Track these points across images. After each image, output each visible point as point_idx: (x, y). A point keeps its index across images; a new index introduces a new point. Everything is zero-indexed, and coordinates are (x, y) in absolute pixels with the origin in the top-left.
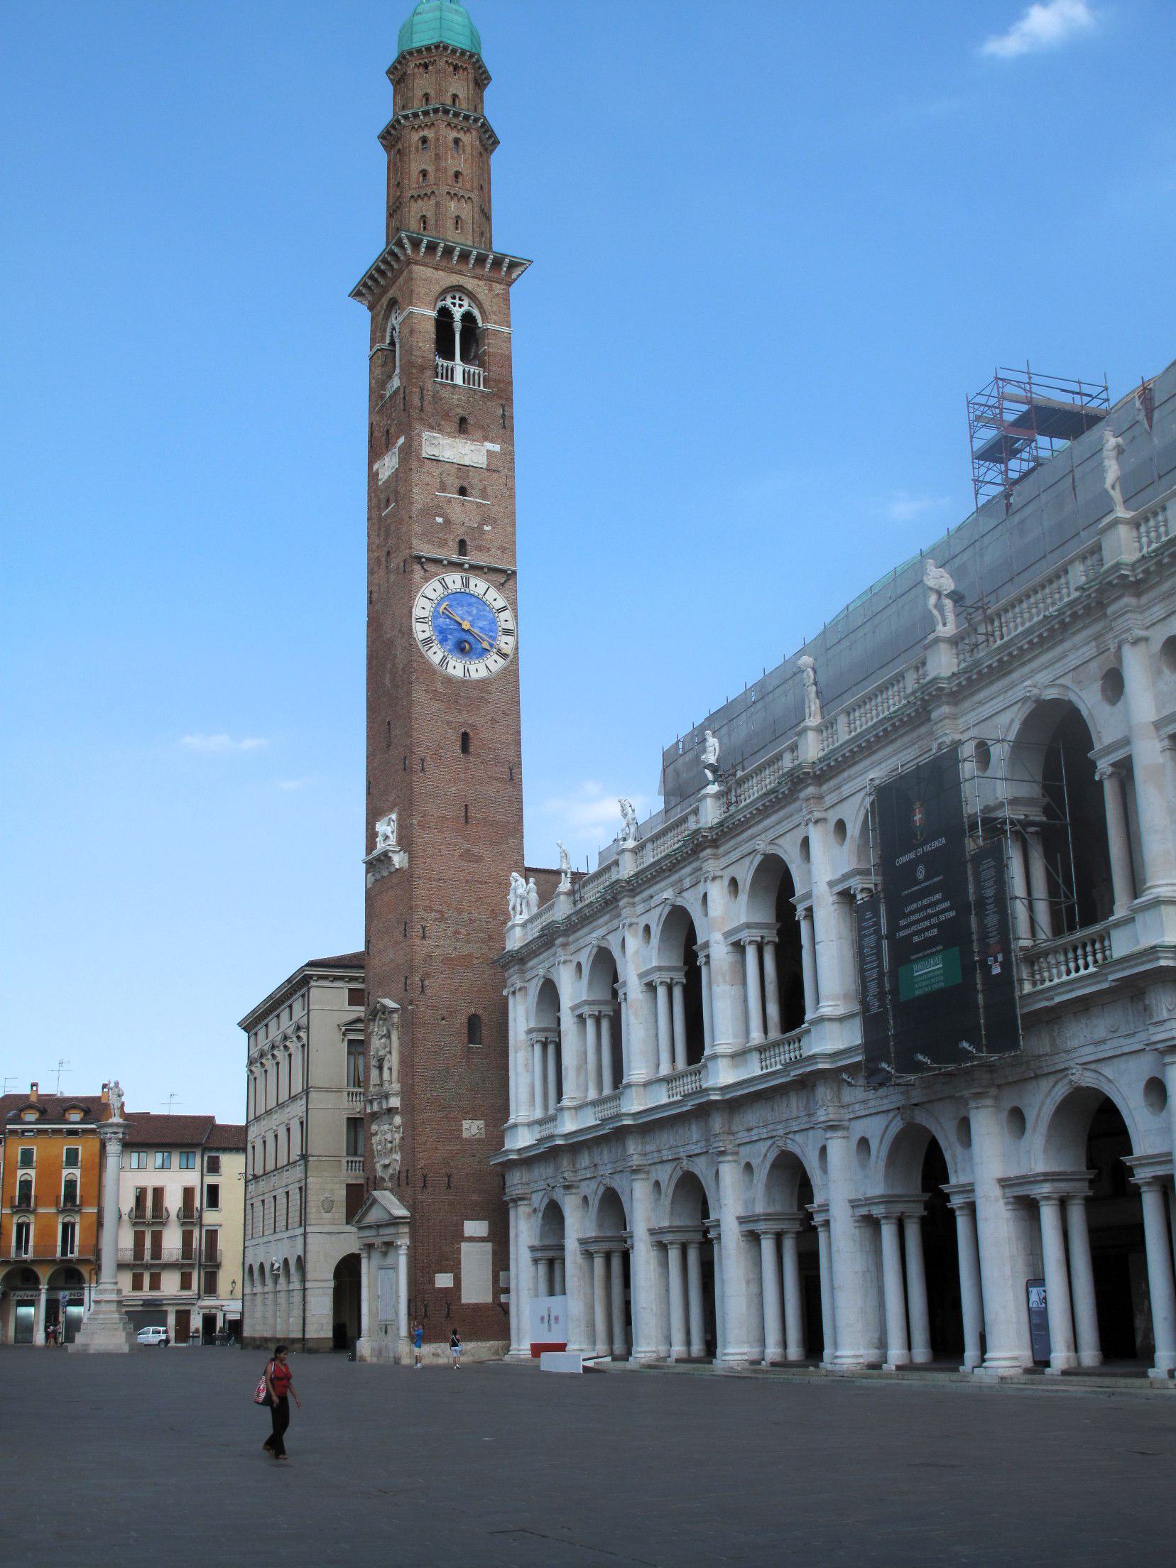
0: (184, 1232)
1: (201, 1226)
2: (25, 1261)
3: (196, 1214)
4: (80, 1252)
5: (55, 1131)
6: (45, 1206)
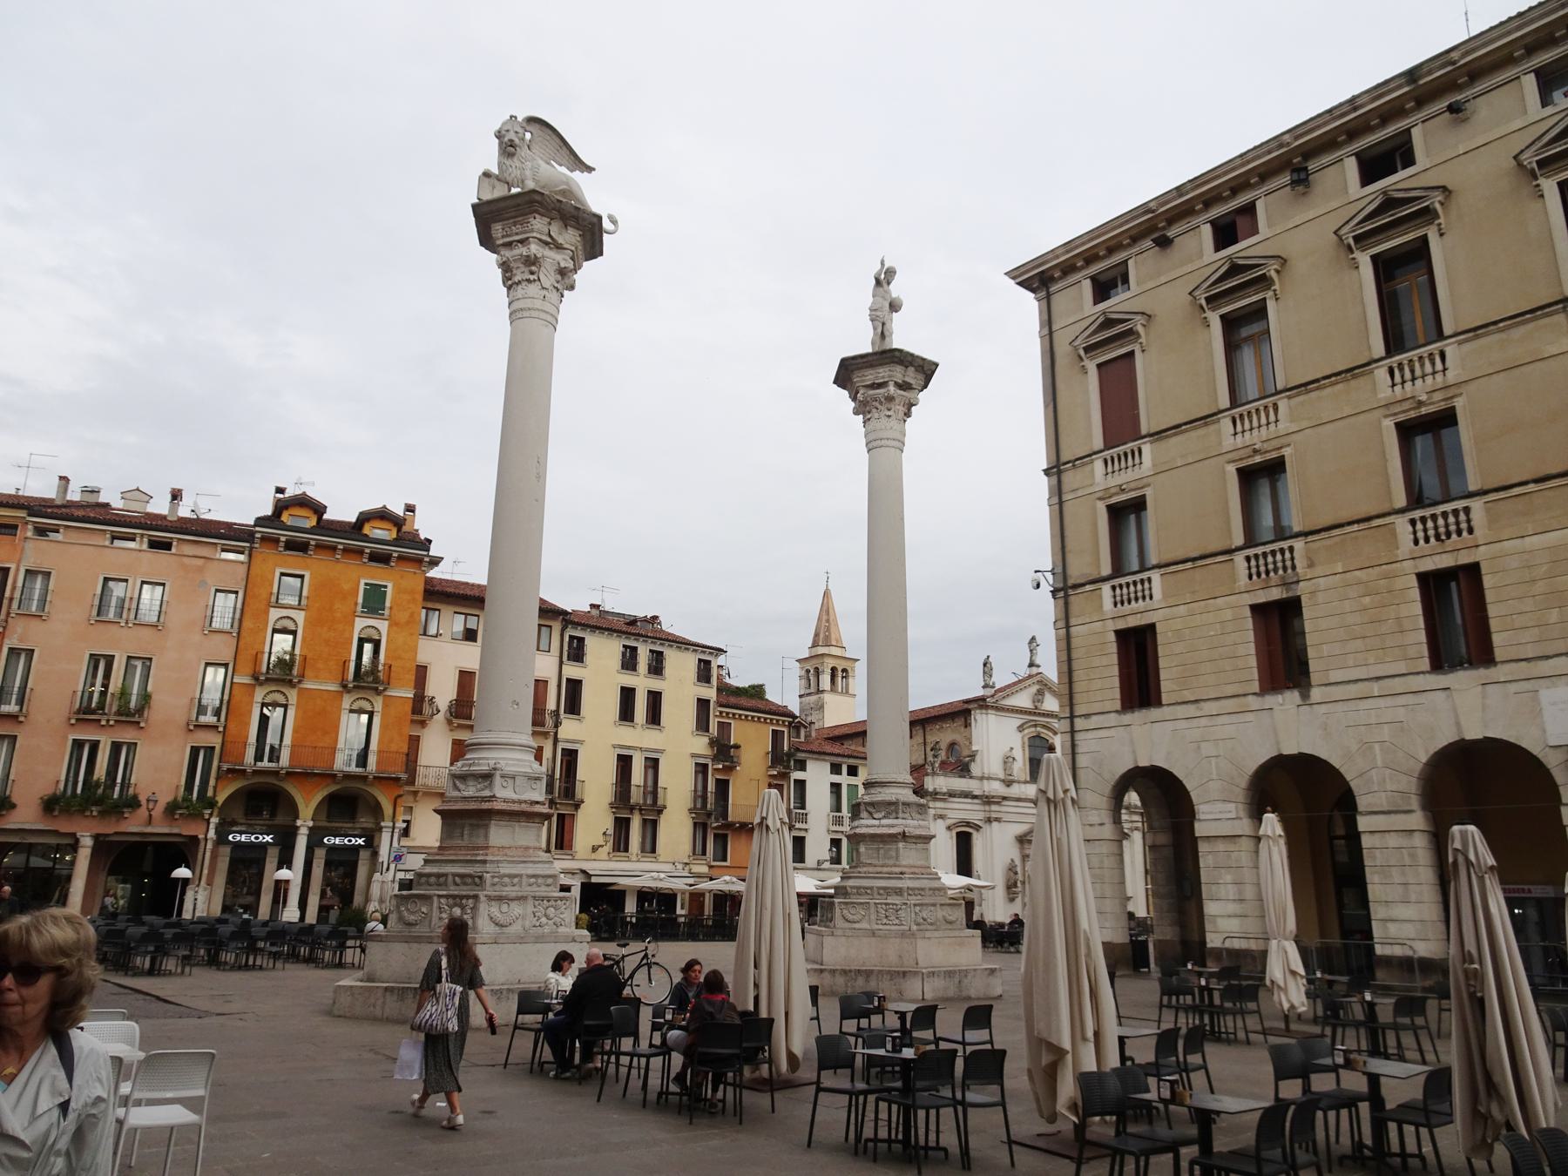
1: (556, 740)
2: (275, 773)
3: (549, 722)
4: (378, 763)
5: (347, 551)
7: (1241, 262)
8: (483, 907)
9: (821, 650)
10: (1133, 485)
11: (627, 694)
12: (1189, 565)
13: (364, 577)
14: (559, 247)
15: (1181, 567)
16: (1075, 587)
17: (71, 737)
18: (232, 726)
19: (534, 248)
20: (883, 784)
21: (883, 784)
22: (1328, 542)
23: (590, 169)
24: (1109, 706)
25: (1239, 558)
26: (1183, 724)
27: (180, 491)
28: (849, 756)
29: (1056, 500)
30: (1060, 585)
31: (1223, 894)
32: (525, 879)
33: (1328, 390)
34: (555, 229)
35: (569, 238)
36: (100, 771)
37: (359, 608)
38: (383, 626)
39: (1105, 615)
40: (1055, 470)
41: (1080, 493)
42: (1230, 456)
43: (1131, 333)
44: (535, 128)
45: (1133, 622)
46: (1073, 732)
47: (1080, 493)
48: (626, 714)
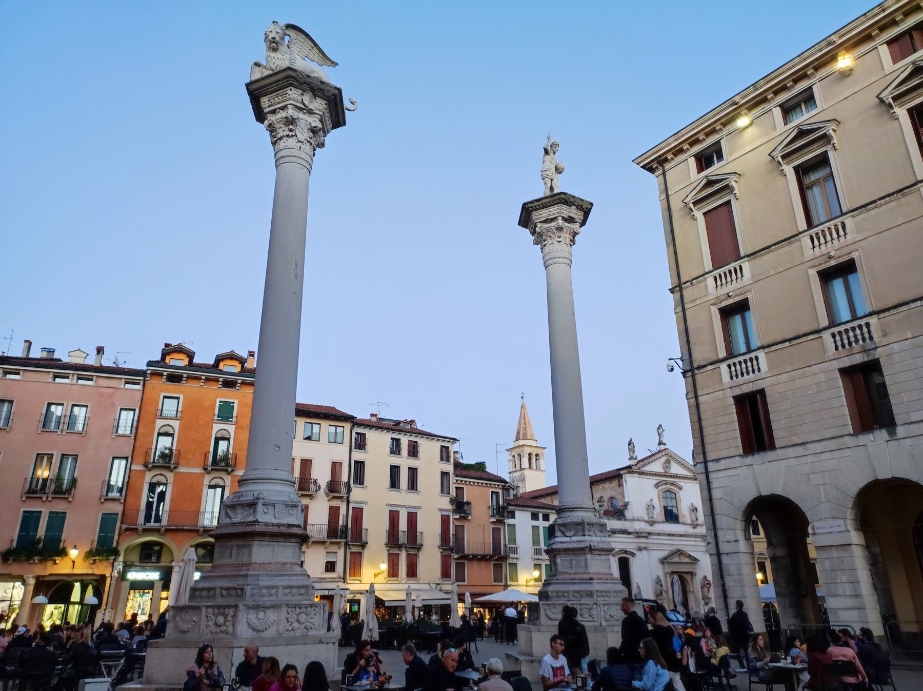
0: (331, 508)
3: (344, 490)
6: (187, 465)
7: (805, 128)
8: (242, 615)
9: (521, 442)
10: (737, 292)
11: (395, 471)
12: (787, 344)
13: (218, 395)
14: (310, 112)
15: (780, 346)
16: (699, 368)
17: (22, 510)
18: (129, 499)
19: (291, 112)
20: (572, 509)
21: (572, 509)
22: (897, 317)
23: (334, 64)
24: (733, 452)
25: (826, 335)
26: (793, 462)
27: (103, 348)
28: (543, 508)
29: (680, 309)
30: (688, 368)
31: (840, 592)
32: (280, 591)
33: (884, 208)
34: (307, 98)
35: (318, 105)
36: (41, 532)
37: (216, 418)
38: (231, 429)
39: (723, 386)
40: (678, 288)
41: (698, 302)
42: (811, 263)
43: (728, 188)
44: (292, 33)
45: (746, 389)
46: (707, 473)
47: (698, 302)
48: (394, 483)
